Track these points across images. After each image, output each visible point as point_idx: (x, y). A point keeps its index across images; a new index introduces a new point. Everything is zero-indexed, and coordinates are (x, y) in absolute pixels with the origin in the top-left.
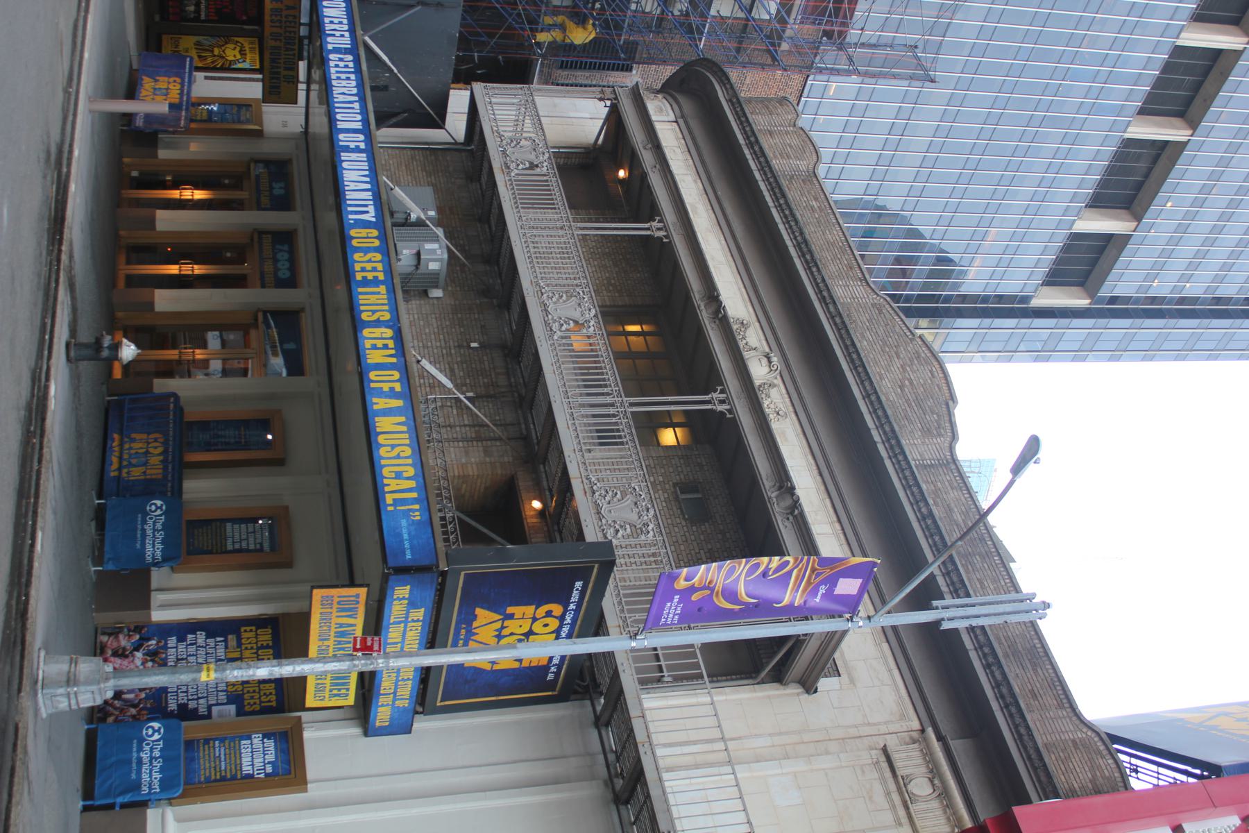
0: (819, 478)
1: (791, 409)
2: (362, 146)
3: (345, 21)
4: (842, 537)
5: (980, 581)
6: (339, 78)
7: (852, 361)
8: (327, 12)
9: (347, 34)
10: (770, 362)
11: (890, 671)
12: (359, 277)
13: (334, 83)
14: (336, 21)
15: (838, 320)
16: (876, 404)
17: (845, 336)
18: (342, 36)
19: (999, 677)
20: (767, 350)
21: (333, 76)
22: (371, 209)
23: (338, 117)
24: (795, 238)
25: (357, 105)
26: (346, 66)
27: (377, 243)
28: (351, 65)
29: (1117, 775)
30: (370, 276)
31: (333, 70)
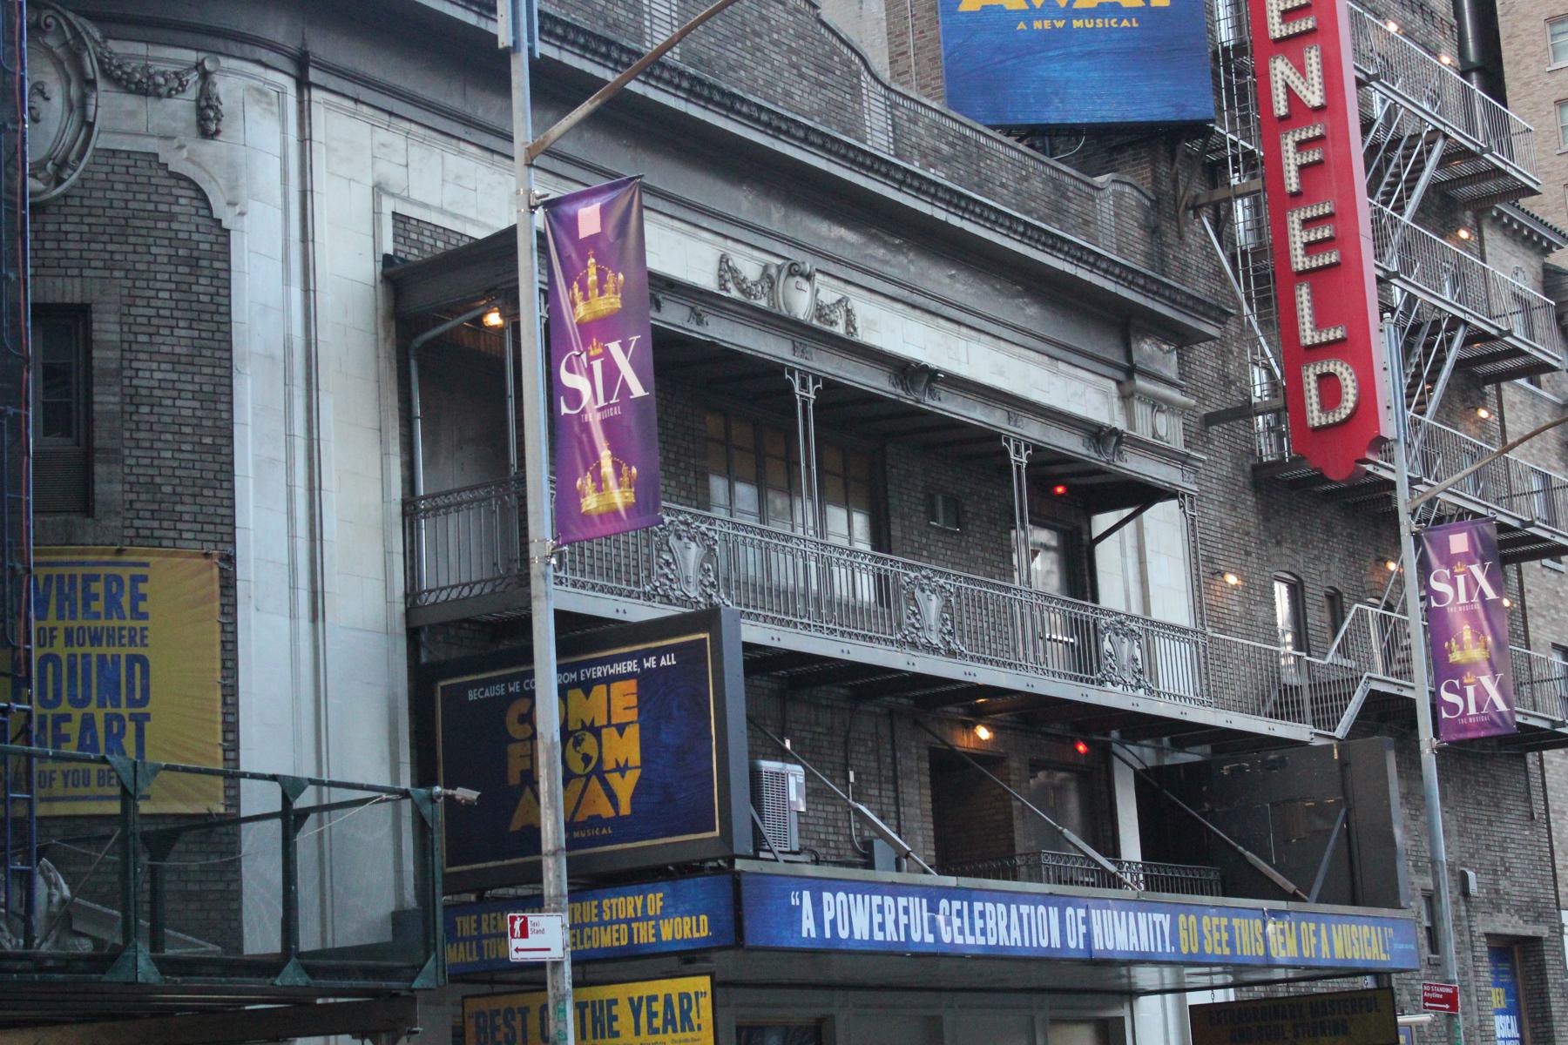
0: (918, 313)
1: (842, 285)
2: (1081, 913)
3: (877, 900)
4: (973, 333)
5: (1002, 185)
6: (984, 932)
7: (862, 165)
8: (861, 931)
9: (902, 901)
10: (808, 277)
11: (1077, 378)
12: (1227, 951)
13: (992, 942)
14: (877, 918)
15: (813, 138)
16: (916, 183)
17: (835, 148)
18: (906, 911)
19: (1141, 282)
20: (780, 262)
21: (981, 941)
22: (1158, 917)
23: (1044, 944)
24: (678, 87)
25: (1024, 909)
26: (960, 914)
27: (1192, 918)
28: (956, 905)
29: (1135, 193)
30: (1225, 936)
31: (970, 940)
